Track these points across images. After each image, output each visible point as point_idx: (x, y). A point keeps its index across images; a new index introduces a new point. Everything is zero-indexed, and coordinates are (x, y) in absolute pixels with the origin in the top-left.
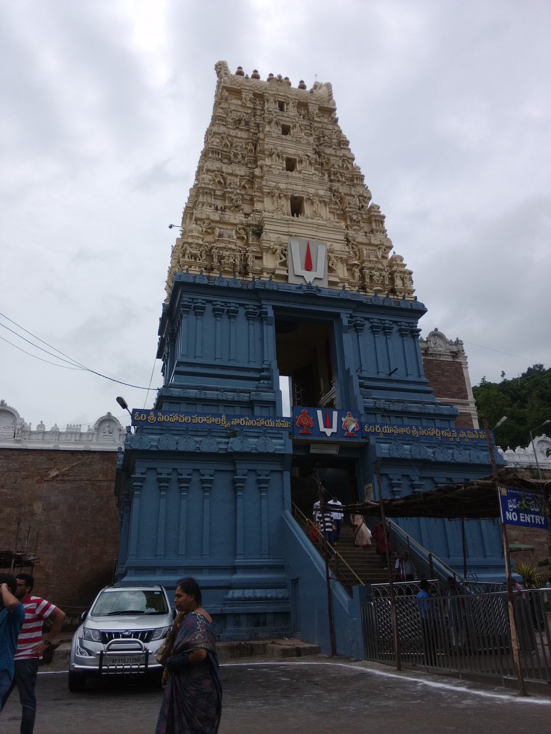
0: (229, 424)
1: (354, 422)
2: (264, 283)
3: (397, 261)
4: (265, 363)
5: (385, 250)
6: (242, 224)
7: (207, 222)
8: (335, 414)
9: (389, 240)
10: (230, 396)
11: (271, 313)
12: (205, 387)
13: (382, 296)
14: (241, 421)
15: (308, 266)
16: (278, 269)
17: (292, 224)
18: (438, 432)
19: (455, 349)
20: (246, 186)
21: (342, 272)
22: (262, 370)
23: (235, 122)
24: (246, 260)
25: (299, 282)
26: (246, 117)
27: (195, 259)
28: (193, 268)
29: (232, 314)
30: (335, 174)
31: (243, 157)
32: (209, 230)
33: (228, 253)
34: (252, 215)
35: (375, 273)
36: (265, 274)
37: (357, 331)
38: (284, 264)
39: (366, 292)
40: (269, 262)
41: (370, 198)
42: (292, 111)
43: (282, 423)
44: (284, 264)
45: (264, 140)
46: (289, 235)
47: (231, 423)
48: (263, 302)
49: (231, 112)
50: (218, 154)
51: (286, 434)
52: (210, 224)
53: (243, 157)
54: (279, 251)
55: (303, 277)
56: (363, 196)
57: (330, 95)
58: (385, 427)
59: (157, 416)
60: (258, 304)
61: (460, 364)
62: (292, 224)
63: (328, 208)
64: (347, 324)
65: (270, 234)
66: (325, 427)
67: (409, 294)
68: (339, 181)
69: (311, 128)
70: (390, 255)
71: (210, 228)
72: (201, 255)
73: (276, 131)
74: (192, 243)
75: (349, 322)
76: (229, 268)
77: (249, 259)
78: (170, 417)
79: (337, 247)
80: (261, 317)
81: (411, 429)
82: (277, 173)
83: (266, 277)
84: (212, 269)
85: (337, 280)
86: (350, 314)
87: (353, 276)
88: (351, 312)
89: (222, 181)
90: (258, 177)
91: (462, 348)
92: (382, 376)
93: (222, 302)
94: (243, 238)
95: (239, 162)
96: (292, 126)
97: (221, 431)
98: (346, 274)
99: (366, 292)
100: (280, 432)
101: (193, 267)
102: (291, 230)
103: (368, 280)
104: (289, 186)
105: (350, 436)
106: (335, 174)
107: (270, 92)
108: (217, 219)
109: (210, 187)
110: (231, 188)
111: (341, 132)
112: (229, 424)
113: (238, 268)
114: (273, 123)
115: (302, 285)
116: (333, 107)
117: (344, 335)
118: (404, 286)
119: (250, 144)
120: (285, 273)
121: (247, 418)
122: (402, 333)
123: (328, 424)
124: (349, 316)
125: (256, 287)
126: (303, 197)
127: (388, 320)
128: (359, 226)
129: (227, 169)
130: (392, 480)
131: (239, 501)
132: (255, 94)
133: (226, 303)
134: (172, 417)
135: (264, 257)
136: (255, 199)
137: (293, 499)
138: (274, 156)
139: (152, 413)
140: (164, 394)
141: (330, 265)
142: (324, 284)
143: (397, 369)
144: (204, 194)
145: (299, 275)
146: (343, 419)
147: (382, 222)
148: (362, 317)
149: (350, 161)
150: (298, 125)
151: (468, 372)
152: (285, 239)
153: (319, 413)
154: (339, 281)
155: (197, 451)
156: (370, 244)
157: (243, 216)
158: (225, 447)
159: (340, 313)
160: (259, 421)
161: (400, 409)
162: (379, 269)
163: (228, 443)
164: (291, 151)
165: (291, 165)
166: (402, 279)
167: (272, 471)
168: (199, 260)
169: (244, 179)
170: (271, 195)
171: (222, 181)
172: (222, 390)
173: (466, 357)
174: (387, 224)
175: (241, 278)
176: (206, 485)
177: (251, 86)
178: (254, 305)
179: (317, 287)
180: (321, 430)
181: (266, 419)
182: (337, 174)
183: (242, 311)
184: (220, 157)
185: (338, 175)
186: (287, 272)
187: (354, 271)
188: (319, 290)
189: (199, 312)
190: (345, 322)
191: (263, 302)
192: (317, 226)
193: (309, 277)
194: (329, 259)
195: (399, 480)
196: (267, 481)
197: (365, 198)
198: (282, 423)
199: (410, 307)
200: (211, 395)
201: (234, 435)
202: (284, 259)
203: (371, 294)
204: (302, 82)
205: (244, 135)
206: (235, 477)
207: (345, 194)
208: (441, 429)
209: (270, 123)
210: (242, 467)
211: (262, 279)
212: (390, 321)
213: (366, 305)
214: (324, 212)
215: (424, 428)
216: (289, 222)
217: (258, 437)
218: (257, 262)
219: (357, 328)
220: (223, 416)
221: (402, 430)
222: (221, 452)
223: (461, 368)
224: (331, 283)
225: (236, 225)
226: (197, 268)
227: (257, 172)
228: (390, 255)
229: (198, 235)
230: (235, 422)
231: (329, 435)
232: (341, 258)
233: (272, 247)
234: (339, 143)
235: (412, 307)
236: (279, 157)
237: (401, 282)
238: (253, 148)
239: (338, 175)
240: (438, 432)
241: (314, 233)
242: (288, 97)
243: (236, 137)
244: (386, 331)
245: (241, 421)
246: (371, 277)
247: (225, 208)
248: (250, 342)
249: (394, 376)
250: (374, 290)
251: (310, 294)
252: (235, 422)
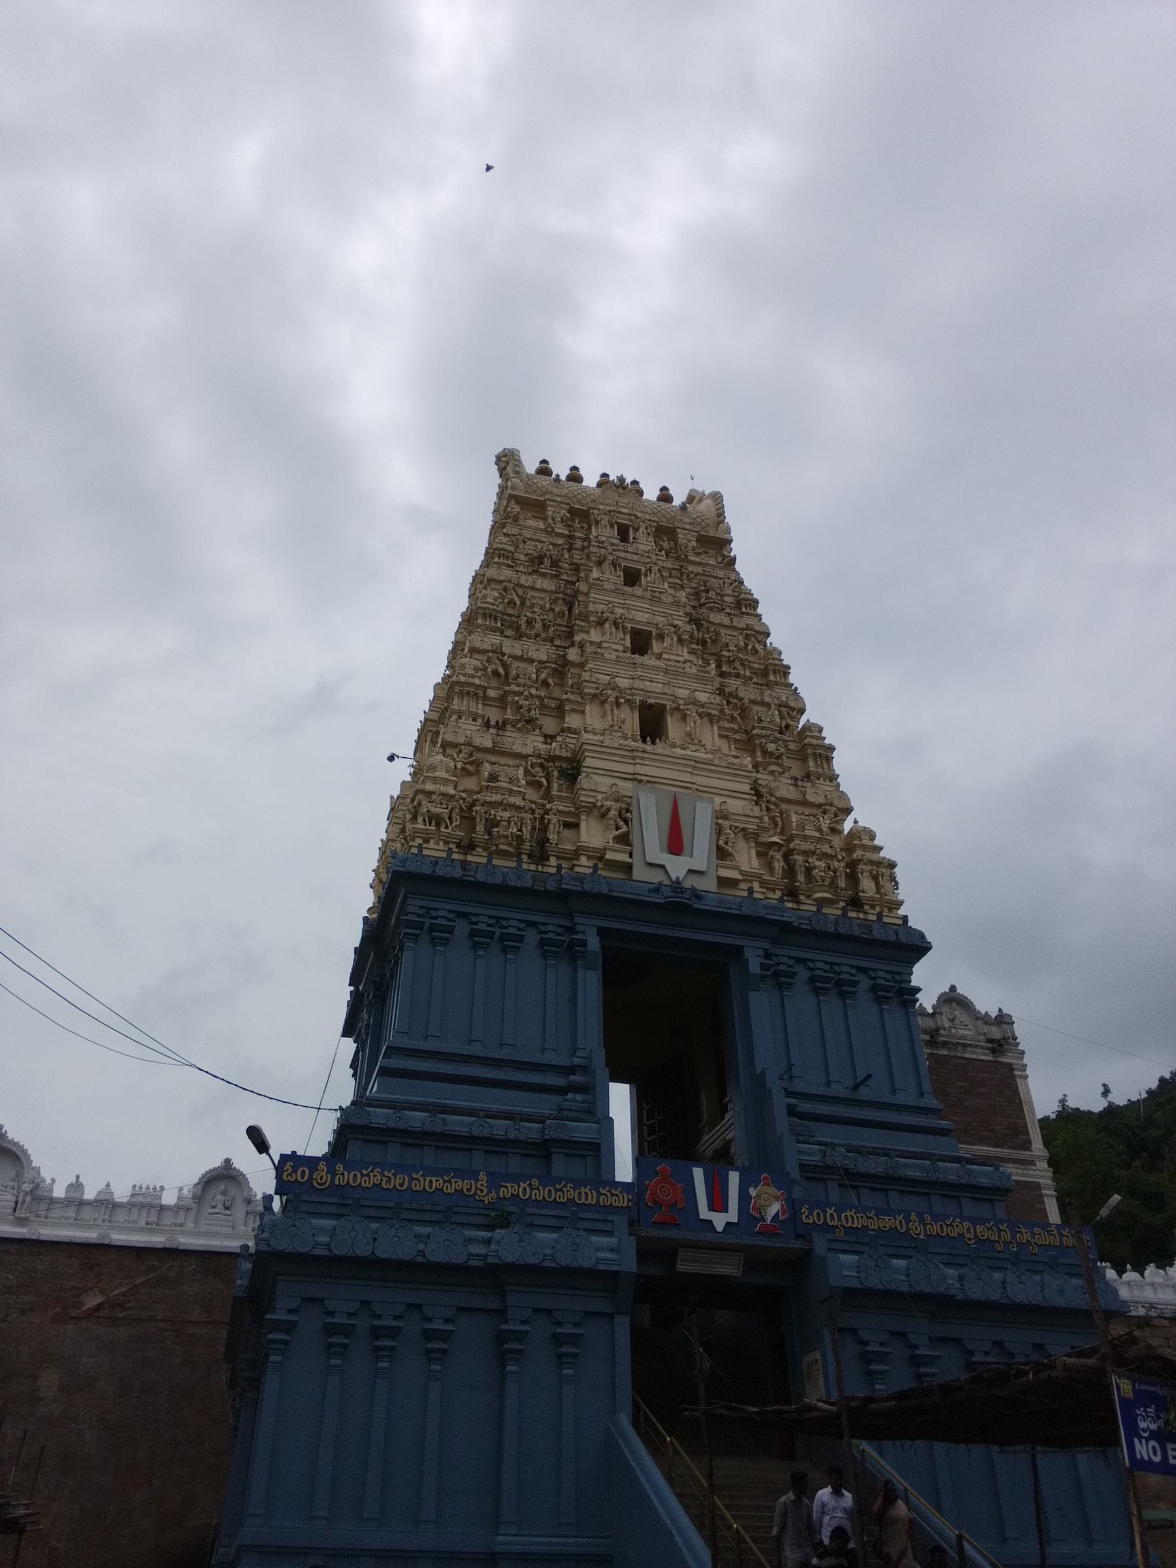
0: (493, 1195)
1: (777, 1198)
2: (581, 878)
3: (862, 839)
4: (579, 1053)
5: (836, 816)
6: (539, 756)
7: (466, 750)
8: (734, 1178)
9: (843, 796)
10: (499, 1128)
11: (594, 943)
12: (445, 1105)
13: (834, 911)
14: (521, 1189)
15: (676, 844)
16: (611, 850)
17: (643, 758)
18: (968, 1229)
19: (996, 1033)
20: (550, 681)
21: (746, 859)
22: (572, 1070)
23: (532, 561)
24: (544, 828)
25: (656, 877)
26: (554, 552)
27: (438, 825)
28: (432, 844)
29: (510, 944)
30: (730, 662)
31: (545, 627)
32: (469, 767)
33: (506, 815)
34: (559, 739)
35: (817, 863)
36: (583, 860)
37: (780, 987)
38: (624, 839)
39: (798, 903)
40: (592, 834)
41: (802, 711)
42: (644, 543)
43: (613, 1195)
44: (624, 839)
45: (587, 594)
46: (635, 780)
47: (498, 1193)
48: (577, 920)
49: (524, 542)
50: (496, 620)
51: (621, 1222)
52: (471, 755)
53: (544, 625)
54: (613, 813)
55: (663, 867)
56: (787, 706)
57: (721, 514)
58: (848, 1213)
59: (332, 1172)
60: (567, 923)
61: (1010, 1067)
62: (643, 758)
63: (716, 728)
64: (758, 971)
65: (596, 778)
66: (712, 1208)
67: (890, 910)
68: (738, 676)
69: (682, 574)
70: (848, 825)
71: (471, 763)
72: (450, 818)
73: (612, 578)
74: (434, 793)
75: (764, 967)
76: (509, 845)
77: (551, 827)
78: (363, 1175)
79: (736, 806)
80: (573, 952)
81: (908, 1221)
82: (613, 657)
83: (584, 865)
84: (470, 847)
86: (766, 950)
87: (771, 869)
88: (767, 946)
89: (501, 670)
90: (573, 664)
91: (1013, 1032)
92: (837, 1090)
93: (490, 917)
94: (540, 785)
95: (537, 635)
96: (643, 570)
97: (476, 1211)
98: (755, 863)
99: (798, 903)
100: (610, 1218)
101: (432, 841)
102: (639, 769)
103: (801, 878)
104: (638, 684)
105: (769, 1232)
106: (730, 662)
107: (601, 507)
108: (488, 744)
109: (477, 681)
110: (518, 685)
111: (742, 583)
112: (493, 1195)
113: (527, 846)
114: (606, 564)
115: (660, 884)
116: (726, 536)
117: (753, 997)
118: (878, 892)
119: (561, 602)
120: (625, 858)
121: (535, 1182)
122: (879, 994)
123: (718, 1203)
124: (761, 953)
125: (564, 886)
126: (665, 706)
128: (781, 766)
129: (511, 647)
130: (866, 1343)
132: (572, 511)
133: (498, 918)
134: (368, 1175)
135: (583, 825)
136: (567, 708)
137: (636, 1387)
138: (607, 625)
139: (322, 1166)
140: (354, 1121)
141: (721, 843)
142: (708, 885)
143: (870, 1076)
144: (462, 695)
145: (655, 862)
146: (753, 1192)
147: (829, 760)
148: (789, 957)
149: (760, 638)
150: (656, 568)
151: (1027, 1088)
152: (626, 787)
153: (698, 1174)
154: (740, 877)
155: (420, 1259)
156: (805, 803)
157: (542, 739)
158: (483, 1251)
159: (742, 947)
160: (561, 1190)
161: (880, 1169)
162: (825, 856)
163: (488, 1242)
164: (642, 615)
165: (640, 642)
166: (875, 878)
167: (588, 1314)
168: (447, 827)
169: (545, 668)
170: (599, 699)
171: (501, 670)
172: (482, 1114)
173: (1023, 1053)
174: (840, 763)
175: (533, 867)
177: (566, 495)
178: (559, 926)
179: (693, 889)
180: (702, 1217)
181: (578, 1184)
182: (733, 661)
183: (532, 937)
184: (499, 625)
185: (737, 664)
186: (631, 857)
187: (772, 857)
188: (697, 895)
189: (440, 936)
190: (754, 967)
191: (577, 920)
192: (693, 763)
193: (677, 867)
194: (719, 831)
195: (882, 1344)
196: (575, 1339)
197: (793, 709)
198: (613, 1195)
199: (893, 938)
200: (457, 1124)
201: (505, 1224)
202: (624, 829)
203: (809, 907)
204: (664, 489)
205: (548, 585)
206: (503, 1327)
207: (752, 702)
208: (975, 1221)
209: (600, 563)
211: (577, 869)
212: (851, 966)
213: (799, 931)
214: (709, 735)
215: (936, 1218)
216: (635, 754)
217: (557, 1229)
218: (567, 833)
219: (780, 980)
220: (481, 1176)
221: (888, 1222)
222: (472, 1263)
223: (1013, 1078)
224: (723, 882)
225: (525, 757)
226: (441, 843)
227: (573, 654)
228: (848, 825)
229: (446, 775)
230: (508, 1190)
231: (720, 1227)
232: (744, 829)
233: (599, 804)
234: (738, 604)
235: (897, 938)
236: (617, 628)
237: (872, 884)
238: (565, 609)
239: (737, 664)
240: (968, 1229)
241: (687, 778)
242: (637, 517)
243: (533, 588)
244: (844, 990)
245: (521, 1189)
246: (809, 870)
247: (505, 723)
248: (548, 1005)
249: (864, 1093)
250: (816, 900)
251: (678, 904)
252: (508, 1190)
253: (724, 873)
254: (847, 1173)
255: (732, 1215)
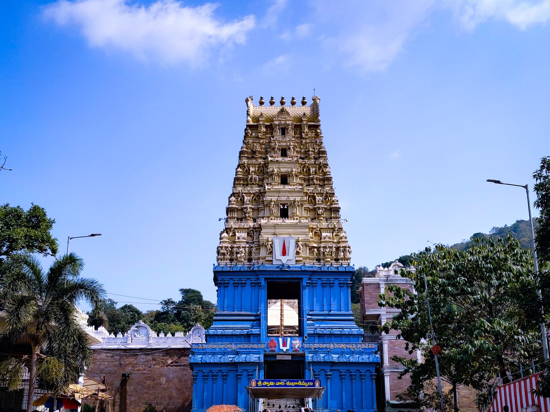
10: (238, 332)
21: (305, 253)
40: (263, 253)
80: (258, 285)
85: (301, 259)
103: (322, 255)
123: (285, 345)
127: (332, 278)
131: (239, 385)
141: (298, 250)
142: (292, 263)
146: (293, 342)
176: (225, 377)
193: (284, 259)
210: (240, 369)
221: (325, 346)
224: (296, 261)
246: (324, 252)
253: (297, 259)
254: (320, 334)
255: (288, 347)
